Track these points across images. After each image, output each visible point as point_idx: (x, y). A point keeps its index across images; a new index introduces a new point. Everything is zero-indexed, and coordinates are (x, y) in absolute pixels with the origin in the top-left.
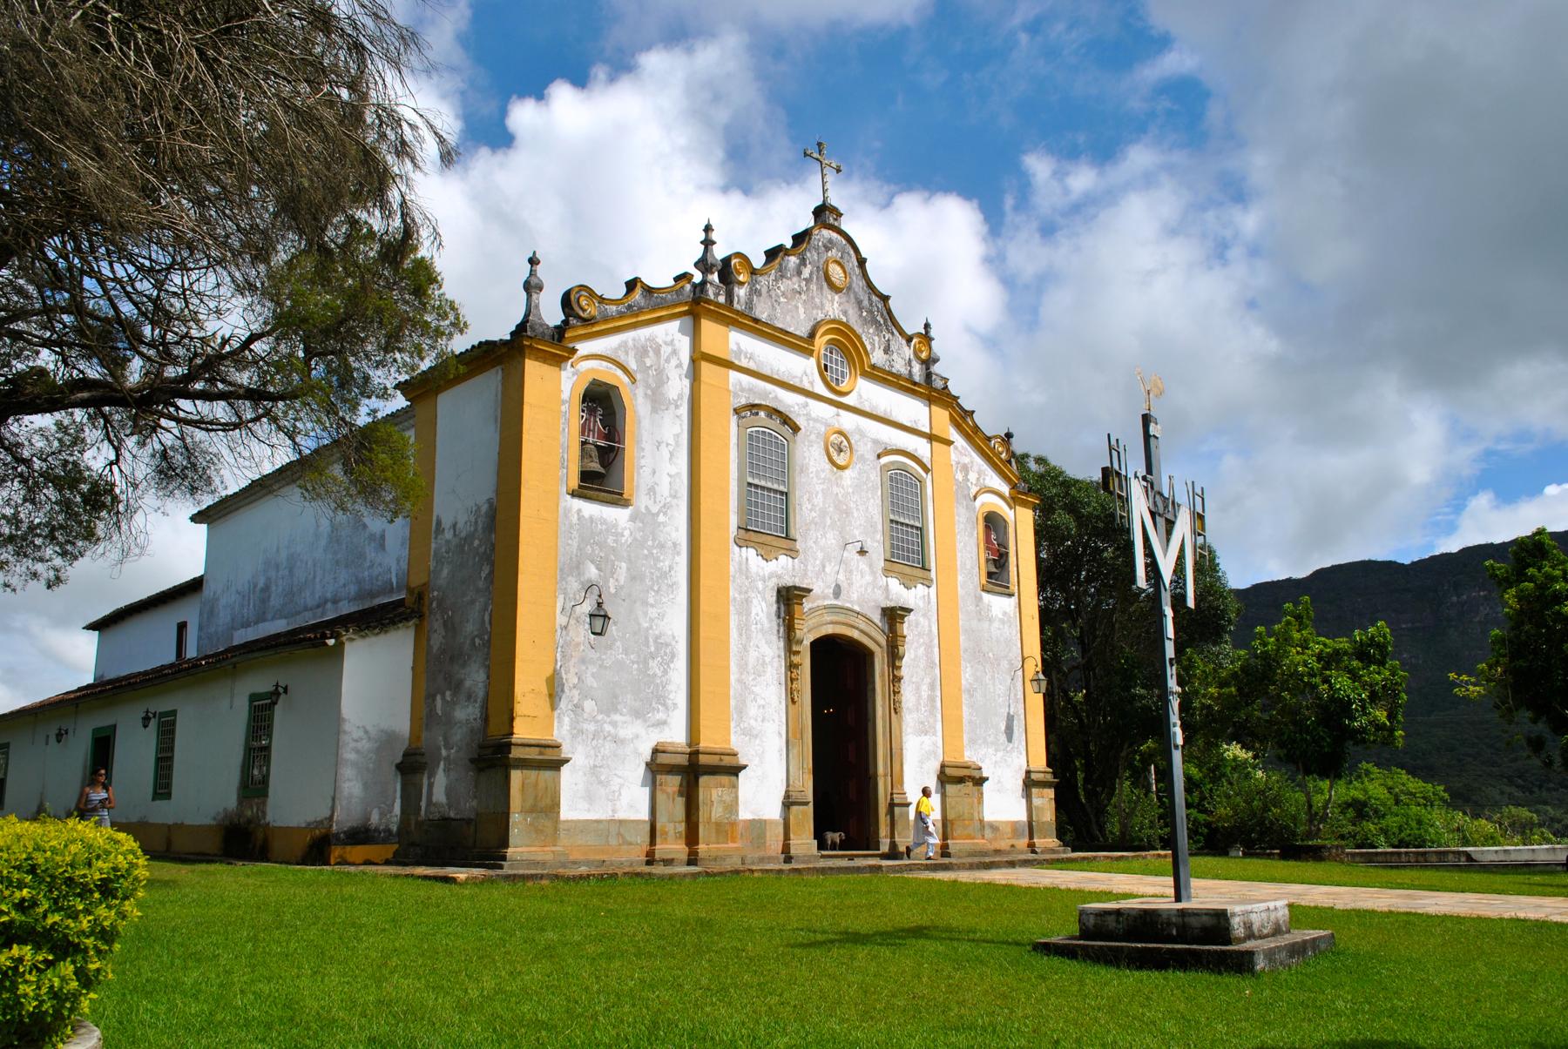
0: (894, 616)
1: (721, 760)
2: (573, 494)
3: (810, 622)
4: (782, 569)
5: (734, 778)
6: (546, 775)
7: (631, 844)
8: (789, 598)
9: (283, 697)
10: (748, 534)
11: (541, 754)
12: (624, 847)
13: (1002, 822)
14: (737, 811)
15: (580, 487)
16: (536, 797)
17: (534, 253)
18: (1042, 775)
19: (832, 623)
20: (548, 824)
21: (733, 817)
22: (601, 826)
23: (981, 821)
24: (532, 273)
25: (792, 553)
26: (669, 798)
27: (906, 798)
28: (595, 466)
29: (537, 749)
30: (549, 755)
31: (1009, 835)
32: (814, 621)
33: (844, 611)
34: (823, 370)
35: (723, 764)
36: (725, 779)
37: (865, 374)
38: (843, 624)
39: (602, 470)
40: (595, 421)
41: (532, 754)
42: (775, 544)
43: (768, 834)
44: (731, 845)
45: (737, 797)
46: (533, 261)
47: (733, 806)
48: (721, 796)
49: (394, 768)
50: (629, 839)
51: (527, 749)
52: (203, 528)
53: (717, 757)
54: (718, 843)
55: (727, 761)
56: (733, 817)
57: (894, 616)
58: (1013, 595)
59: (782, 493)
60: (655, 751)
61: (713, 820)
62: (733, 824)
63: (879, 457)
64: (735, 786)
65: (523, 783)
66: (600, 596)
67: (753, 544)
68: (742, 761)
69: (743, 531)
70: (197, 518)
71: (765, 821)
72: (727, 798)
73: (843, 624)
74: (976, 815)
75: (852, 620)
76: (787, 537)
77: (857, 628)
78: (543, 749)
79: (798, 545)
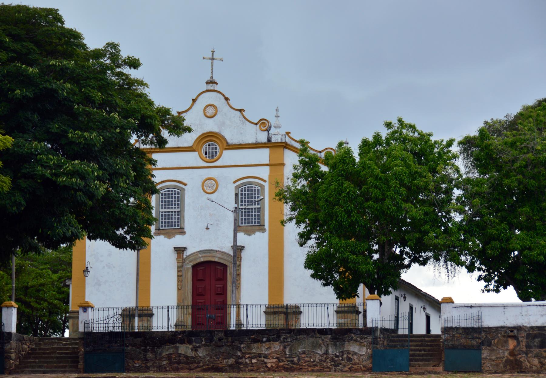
3: (190, 258)
4: (178, 241)
5: (149, 318)
8: (180, 250)
19: (202, 257)
32: (193, 257)
37: (226, 149)
38: (209, 256)
51: (74, 313)
57: (238, 250)
63: (234, 182)
64: (150, 321)
69: (157, 231)
73: (209, 256)
75: (214, 254)
79: (185, 230)
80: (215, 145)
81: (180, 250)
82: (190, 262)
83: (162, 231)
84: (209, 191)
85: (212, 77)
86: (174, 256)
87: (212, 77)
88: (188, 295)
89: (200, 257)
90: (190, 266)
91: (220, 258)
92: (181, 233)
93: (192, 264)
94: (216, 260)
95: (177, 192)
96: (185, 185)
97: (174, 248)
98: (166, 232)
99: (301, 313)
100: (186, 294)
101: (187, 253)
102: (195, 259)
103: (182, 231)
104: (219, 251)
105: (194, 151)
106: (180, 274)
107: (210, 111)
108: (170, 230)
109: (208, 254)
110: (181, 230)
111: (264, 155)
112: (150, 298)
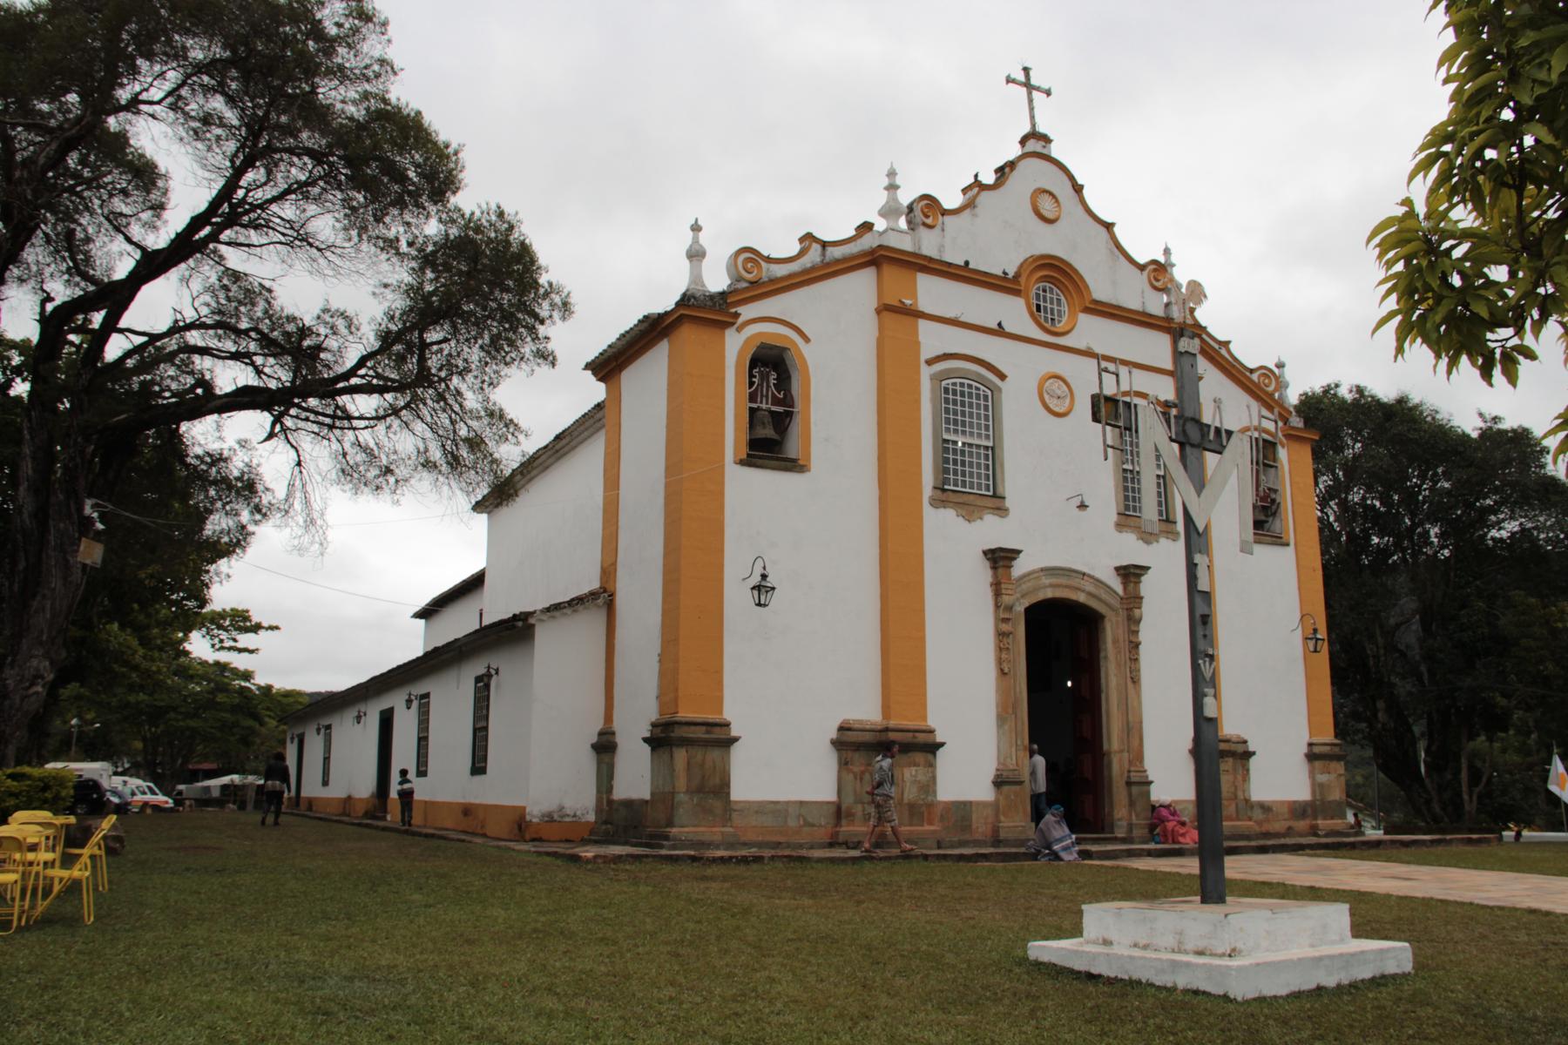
0: (1131, 574)
1: (914, 737)
2: (742, 463)
3: (1024, 586)
4: (992, 531)
5: (930, 756)
6: (714, 754)
7: (813, 825)
8: (1000, 558)
9: (494, 678)
10: (944, 495)
11: (708, 732)
12: (806, 829)
13: (1276, 802)
14: (935, 792)
15: (748, 455)
16: (703, 777)
17: (697, 220)
18: (1328, 748)
19: (1051, 586)
20: (718, 805)
21: (930, 798)
22: (779, 807)
23: (1247, 801)
24: (696, 241)
25: (1001, 511)
26: (856, 778)
27: (1147, 777)
28: (768, 432)
29: (704, 728)
30: (718, 734)
31: (1286, 816)
32: (1029, 584)
33: (1067, 573)
34: (1036, 311)
35: (916, 741)
36: (919, 757)
37: (1087, 310)
39: (776, 437)
40: (768, 386)
41: (700, 733)
42: (979, 503)
43: (974, 817)
44: (927, 827)
45: (934, 778)
46: (696, 228)
47: (929, 786)
48: (915, 776)
49: (589, 746)
50: (810, 820)
51: (693, 728)
52: (483, 518)
53: (911, 734)
54: (911, 825)
55: (921, 738)
56: (930, 798)
57: (1131, 574)
58: (1288, 545)
59: (986, 448)
60: (841, 729)
61: (906, 801)
62: (931, 806)
64: (931, 765)
65: (688, 763)
66: (764, 568)
67: (951, 505)
68: (939, 739)
69: (939, 492)
70: (478, 507)
71: (971, 802)
72: (921, 777)
73: (1067, 587)
74: (1240, 794)
75: (1076, 582)
76: (995, 496)
77: (1083, 591)
78: (709, 728)
79: (1008, 503)
80: (1057, 295)
81: (1000, 558)
82: (1023, 596)
83: (952, 497)
84: (1057, 409)
85: (1033, 125)
86: (984, 574)
87: (1033, 125)
88: (1021, 692)
89: (1046, 587)
90: (1023, 610)
91: (1090, 594)
92: (999, 509)
93: (1026, 603)
94: (1081, 598)
95: (982, 393)
96: (1002, 377)
97: (985, 553)
98: (961, 500)
99: (1248, 755)
100: (1018, 690)
101: (1020, 567)
102: (1037, 589)
103: (996, 502)
104: (1089, 576)
105: (1016, 292)
106: (1005, 627)
107: (1047, 206)
108: (972, 497)
109: (1064, 581)
110: (996, 502)
111: (1157, 348)
112: (924, 695)
